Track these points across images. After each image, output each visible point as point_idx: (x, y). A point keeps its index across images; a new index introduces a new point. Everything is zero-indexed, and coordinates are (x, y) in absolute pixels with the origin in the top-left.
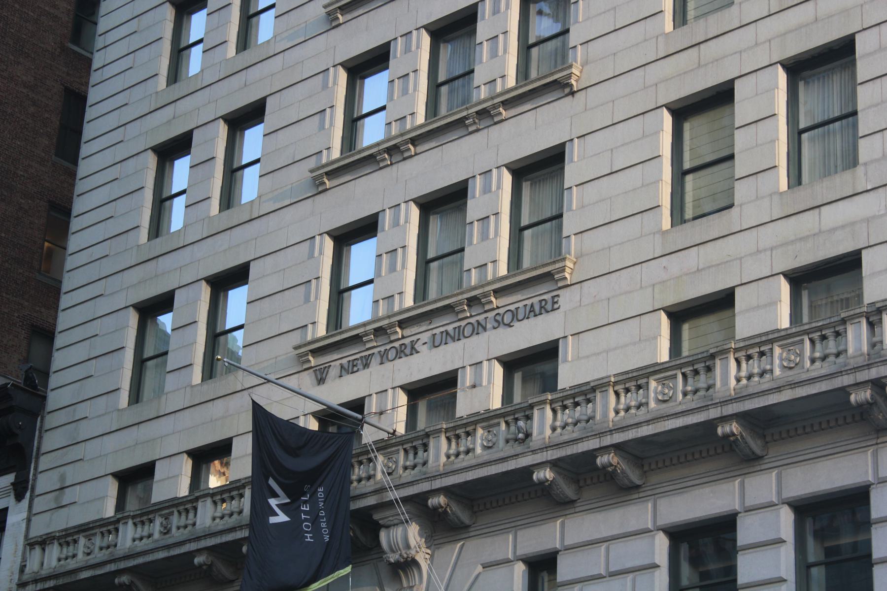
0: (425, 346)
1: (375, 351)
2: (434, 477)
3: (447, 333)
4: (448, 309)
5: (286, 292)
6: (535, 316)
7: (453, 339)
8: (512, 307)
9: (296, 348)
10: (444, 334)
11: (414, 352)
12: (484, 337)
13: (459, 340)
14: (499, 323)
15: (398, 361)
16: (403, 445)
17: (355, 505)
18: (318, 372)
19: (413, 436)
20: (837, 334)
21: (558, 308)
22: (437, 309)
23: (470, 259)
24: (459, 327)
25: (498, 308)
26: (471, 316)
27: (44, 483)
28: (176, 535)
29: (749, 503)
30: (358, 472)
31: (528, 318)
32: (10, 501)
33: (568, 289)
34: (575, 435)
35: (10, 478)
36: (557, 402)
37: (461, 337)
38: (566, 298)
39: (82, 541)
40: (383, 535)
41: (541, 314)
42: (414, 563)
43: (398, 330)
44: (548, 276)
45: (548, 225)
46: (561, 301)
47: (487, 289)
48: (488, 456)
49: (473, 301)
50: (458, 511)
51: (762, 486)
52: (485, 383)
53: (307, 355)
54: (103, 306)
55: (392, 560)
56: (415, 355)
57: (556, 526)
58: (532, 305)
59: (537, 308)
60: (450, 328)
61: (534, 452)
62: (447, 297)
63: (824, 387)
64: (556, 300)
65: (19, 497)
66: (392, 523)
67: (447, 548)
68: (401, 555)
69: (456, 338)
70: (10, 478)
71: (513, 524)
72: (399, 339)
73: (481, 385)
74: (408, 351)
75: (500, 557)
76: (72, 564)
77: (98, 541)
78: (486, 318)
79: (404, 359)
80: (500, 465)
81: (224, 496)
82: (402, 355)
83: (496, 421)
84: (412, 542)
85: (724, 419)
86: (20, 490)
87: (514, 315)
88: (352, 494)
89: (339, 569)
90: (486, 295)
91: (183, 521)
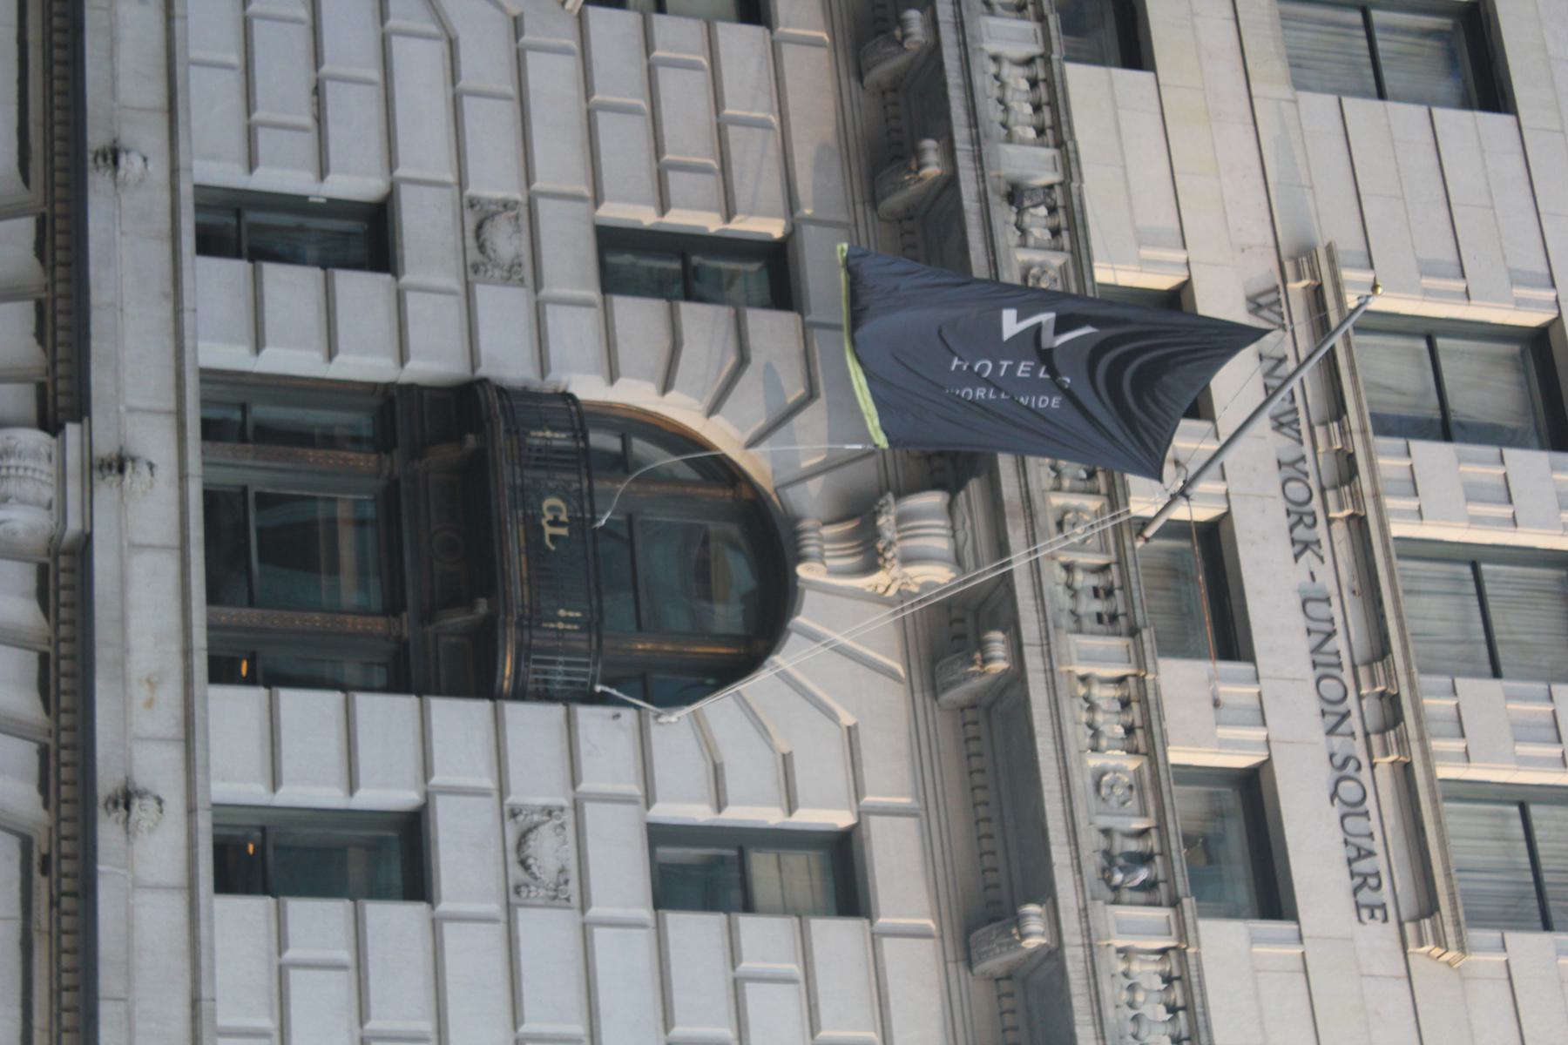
0: (1307, 578)
1: (1307, 449)
2: (1048, 655)
3: (1330, 635)
4: (1381, 650)
5: (1445, 212)
6: (1350, 862)
7: (1316, 650)
8: (1370, 803)
9: (1329, 249)
10: (1327, 627)
11: (1298, 547)
12: (1314, 728)
13: (1315, 665)
14: (1342, 767)
15: (1280, 506)
16: (1118, 563)
17: (1006, 463)
18: (1272, 297)
19: (1136, 594)
21: (1360, 920)
22: (1383, 616)
23: (1478, 692)
24: (1340, 665)
25: (1373, 766)
26: (1360, 698)
30: (1073, 470)
31: (1346, 842)
33: (1398, 946)
34: (1110, 1013)
36: (1180, 963)
37: (1320, 671)
38: (1379, 937)
40: (934, 500)
41: (1352, 875)
42: (871, 565)
43: (1347, 512)
44: (1429, 908)
45: (1525, 860)
46: (1375, 926)
47: (1415, 748)
48: (1082, 784)
49: (1391, 707)
50: (971, 683)
52: (1224, 732)
53: (1314, 277)
55: (882, 521)
56: (1289, 551)
57: (922, 917)
58: (1371, 854)
59: (1363, 866)
60: (1339, 642)
61: (1084, 912)
62: (1405, 648)
64: (1378, 913)
66: (959, 525)
67: (895, 643)
68: (891, 543)
69: (1320, 658)
71: (931, 805)
72: (1326, 510)
73: (1218, 723)
74: (1301, 532)
75: (869, 774)
78: (1353, 734)
79: (1285, 522)
80: (1061, 824)
81: (1046, 110)
82: (1294, 518)
83: (1152, 808)
84: (913, 570)
87: (1355, 809)
88: (1031, 461)
89: (881, 416)
90: (1402, 742)
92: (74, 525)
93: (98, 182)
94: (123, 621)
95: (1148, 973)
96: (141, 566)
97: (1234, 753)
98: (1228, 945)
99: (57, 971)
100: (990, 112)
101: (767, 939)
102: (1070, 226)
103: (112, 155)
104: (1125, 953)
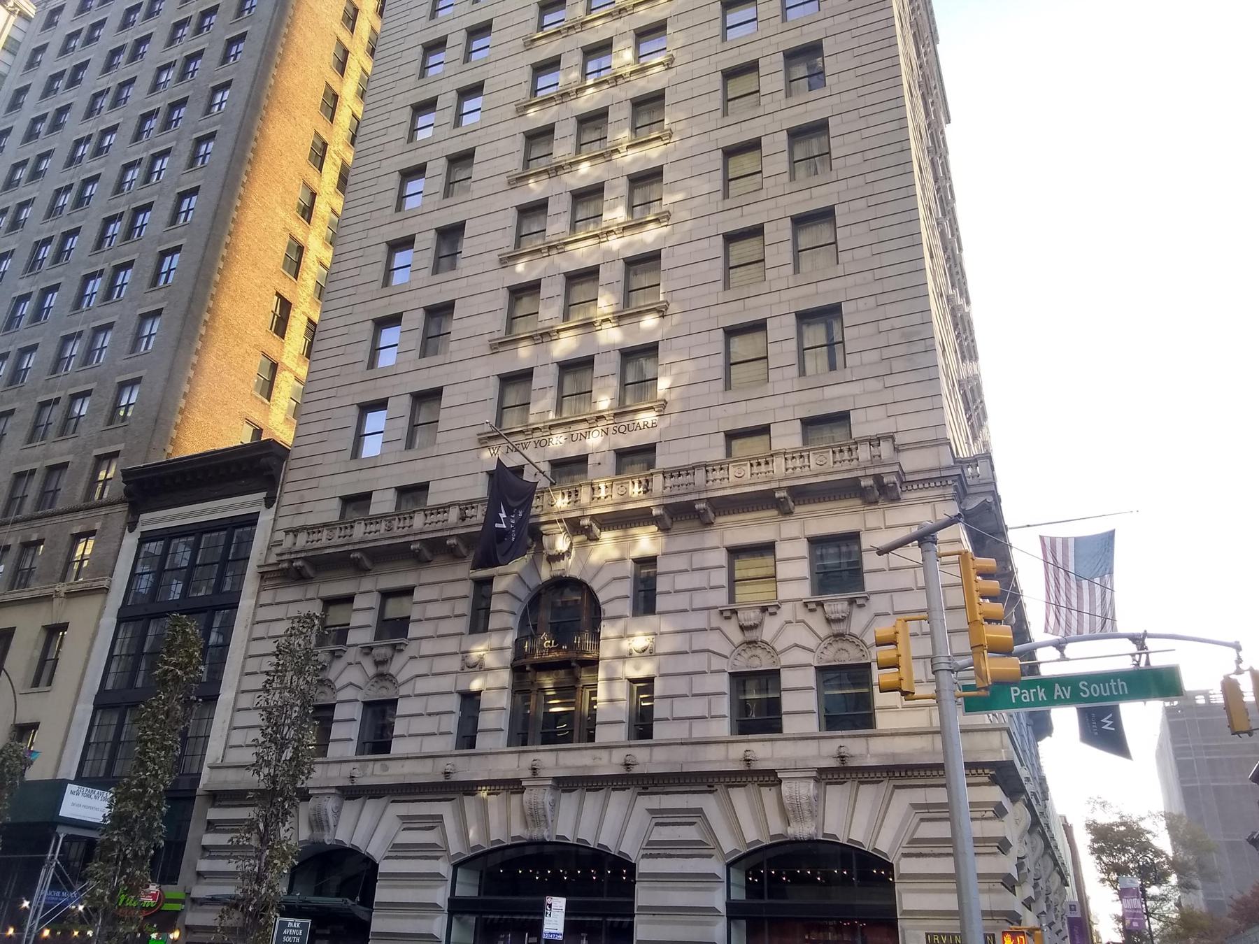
17: (532, 521)
20: (767, 463)
27: (286, 499)
28: (396, 532)
29: (783, 536)
32: (262, 508)
35: (264, 494)
39: (325, 532)
40: (545, 539)
51: (791, 528)
54: (334, 403)
63: (846, 476)
65: (269, 506)
70: (264, 494)
76: (318, 545)
77: (337, 532)
85: (780, 489)
86: (269, 502)
91: (401, 525)
92: (550, 782)
93: (454, 778)
94: (578, 767)
95: (669, 482)
96: (561, 762)
97: (391, 496)
98: (662, 461)
99: (674, 784)
100: (439, 525)
101: (662, 584)
102: (471, 504)
103: (447, 774)
104: (665, 488)
